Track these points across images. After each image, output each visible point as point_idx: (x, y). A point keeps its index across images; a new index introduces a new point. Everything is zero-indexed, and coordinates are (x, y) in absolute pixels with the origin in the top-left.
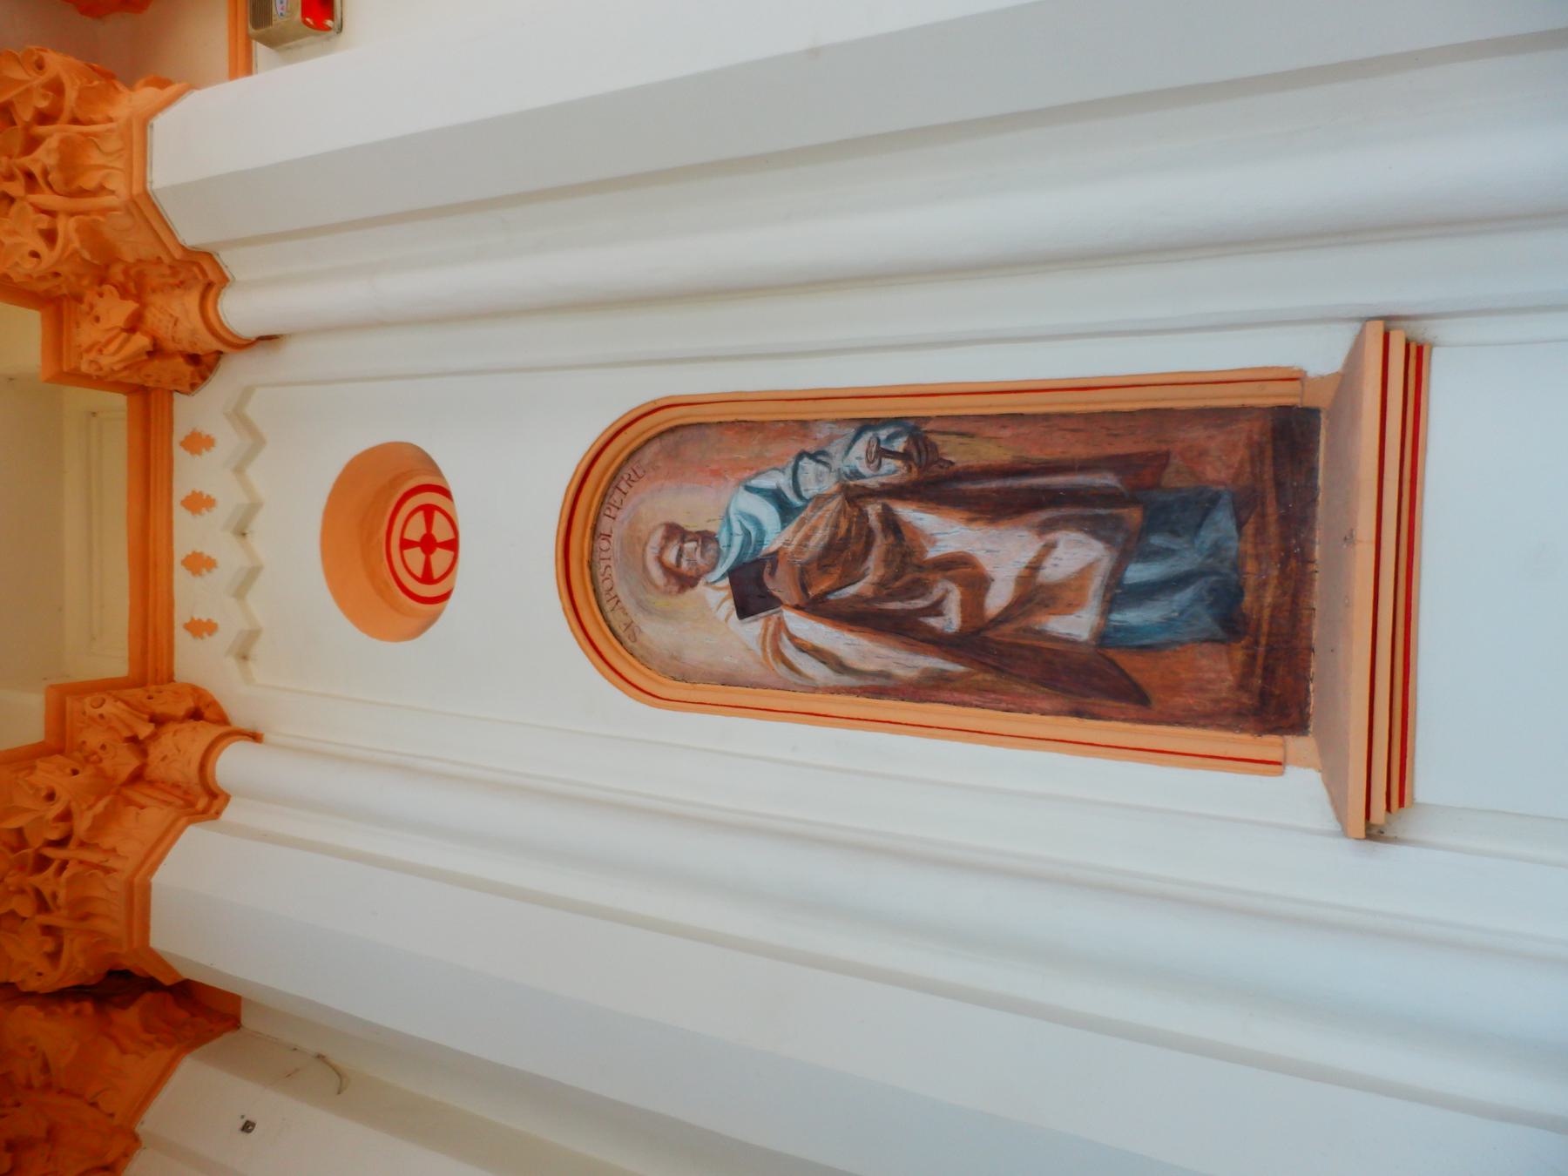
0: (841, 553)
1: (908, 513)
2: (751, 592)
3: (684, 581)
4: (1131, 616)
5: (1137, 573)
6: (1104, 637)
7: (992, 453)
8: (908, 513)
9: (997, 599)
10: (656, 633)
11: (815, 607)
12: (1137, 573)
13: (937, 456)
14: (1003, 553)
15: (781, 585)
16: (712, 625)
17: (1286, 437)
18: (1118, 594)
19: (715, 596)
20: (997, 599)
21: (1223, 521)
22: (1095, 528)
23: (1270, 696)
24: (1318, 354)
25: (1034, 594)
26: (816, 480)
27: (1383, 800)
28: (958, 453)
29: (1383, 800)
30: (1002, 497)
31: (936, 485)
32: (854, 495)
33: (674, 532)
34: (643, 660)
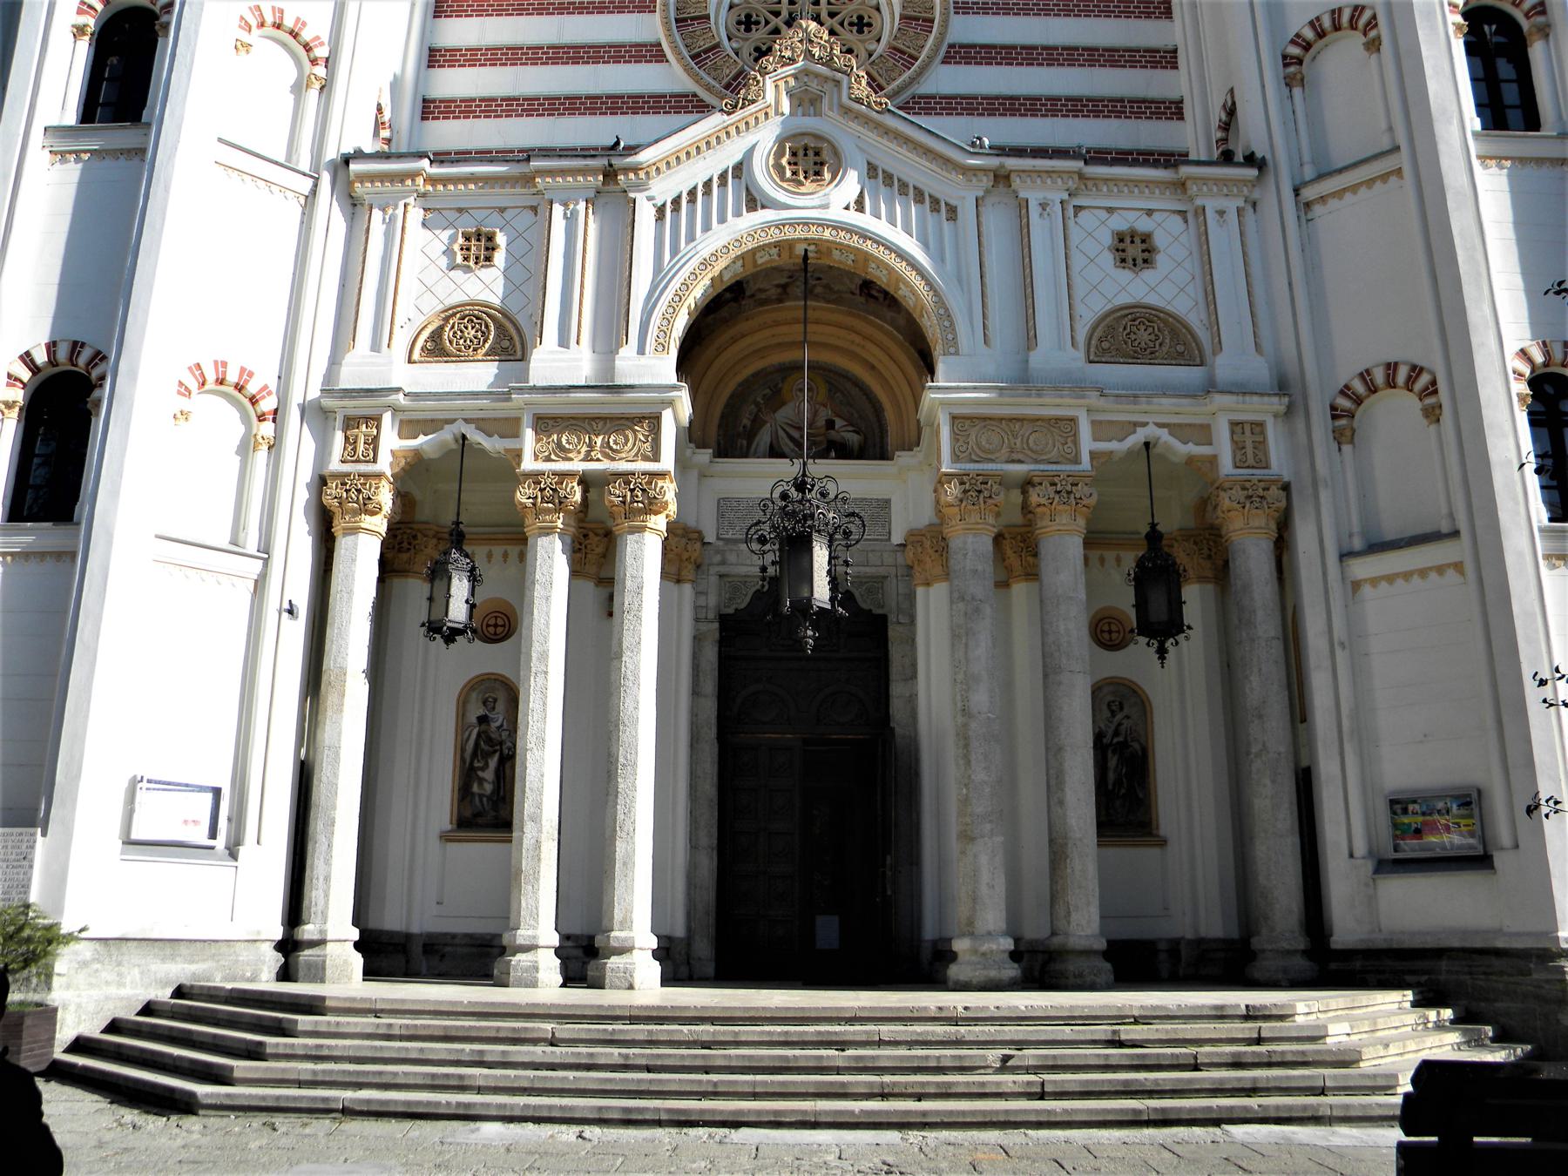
0: (489, 740)
2: (483, 720)
3: (485, 703)
6: (473, 794)
7: (508, 771)
8: (497, 756)
10: (474, 695)
11: (479, 735)
14: (489, 775)
15: (484, 727)
16: (475, 711)
18: (481, 796)
19: (481, 711)
21: (493, 813)
25: (481, 781)
26: (505, 735)
27: (446, 838)
28: (508, 765)
29: (446, 838)
32: (501, 743)
33: (495, 700)
34: (468, 694)
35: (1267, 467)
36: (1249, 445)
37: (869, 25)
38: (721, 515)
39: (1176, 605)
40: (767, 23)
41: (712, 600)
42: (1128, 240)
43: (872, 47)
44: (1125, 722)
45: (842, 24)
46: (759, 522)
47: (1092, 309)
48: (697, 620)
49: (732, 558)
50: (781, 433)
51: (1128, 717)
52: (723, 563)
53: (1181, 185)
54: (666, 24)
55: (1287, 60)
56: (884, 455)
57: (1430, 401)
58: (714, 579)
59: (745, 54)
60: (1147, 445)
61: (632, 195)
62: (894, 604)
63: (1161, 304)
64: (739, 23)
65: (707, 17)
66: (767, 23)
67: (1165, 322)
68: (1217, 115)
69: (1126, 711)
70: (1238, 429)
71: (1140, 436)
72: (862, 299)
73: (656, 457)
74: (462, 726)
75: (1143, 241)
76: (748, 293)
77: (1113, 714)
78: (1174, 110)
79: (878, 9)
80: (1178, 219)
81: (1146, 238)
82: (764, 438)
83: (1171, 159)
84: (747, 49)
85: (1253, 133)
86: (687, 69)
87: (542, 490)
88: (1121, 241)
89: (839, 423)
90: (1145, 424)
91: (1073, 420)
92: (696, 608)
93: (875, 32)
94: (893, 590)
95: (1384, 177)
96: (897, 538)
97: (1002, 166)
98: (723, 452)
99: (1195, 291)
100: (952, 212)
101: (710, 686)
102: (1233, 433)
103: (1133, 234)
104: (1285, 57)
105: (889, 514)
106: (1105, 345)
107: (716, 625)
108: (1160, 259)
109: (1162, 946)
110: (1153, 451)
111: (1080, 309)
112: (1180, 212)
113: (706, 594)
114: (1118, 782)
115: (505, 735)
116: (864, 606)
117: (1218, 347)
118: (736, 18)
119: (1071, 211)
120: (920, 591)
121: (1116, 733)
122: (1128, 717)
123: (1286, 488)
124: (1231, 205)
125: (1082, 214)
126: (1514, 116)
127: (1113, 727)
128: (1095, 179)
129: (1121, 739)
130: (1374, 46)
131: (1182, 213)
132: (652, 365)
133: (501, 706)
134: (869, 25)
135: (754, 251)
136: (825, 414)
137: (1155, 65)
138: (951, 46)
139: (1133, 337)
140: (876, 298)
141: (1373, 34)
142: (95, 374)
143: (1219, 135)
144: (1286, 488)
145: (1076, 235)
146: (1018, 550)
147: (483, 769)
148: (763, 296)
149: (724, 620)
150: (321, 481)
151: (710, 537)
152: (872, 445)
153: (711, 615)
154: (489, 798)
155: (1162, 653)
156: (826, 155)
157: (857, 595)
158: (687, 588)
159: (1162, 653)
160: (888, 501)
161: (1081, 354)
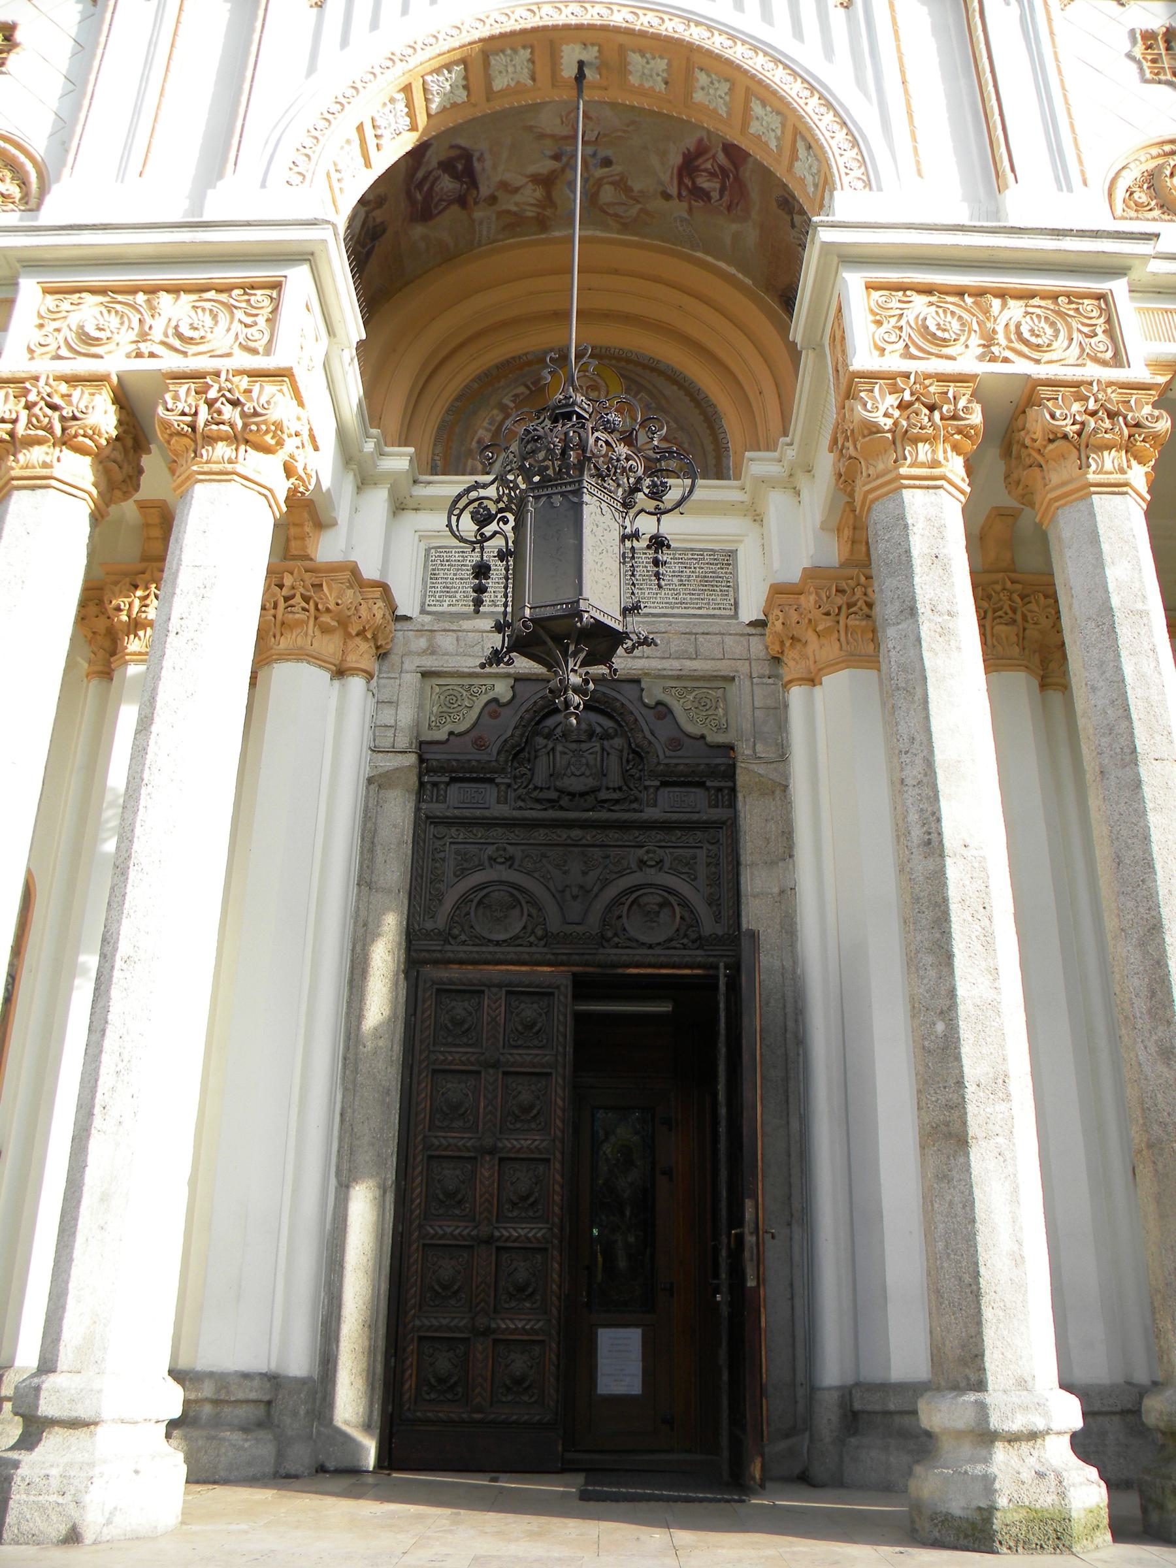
41: (406, 716)
49: (446, 642)
52: (431, 651)
58: (411, 679)
62: (747, 726)
72: (679, 209)
76: (484, 191)
87: (29, 406)
92: (377, 728)
94: (745, 701)
105: (735, 574)
107: (411, 759)
113: (393, 703)
116: (690, 728)
120: (796, 695)
140: (704, 195)
148: (509, 203)
149: (423, 748)
151: (407, 603)
153: (403, 742)
157: (677, 707)
158: (357, 684)
160: (732, 554)
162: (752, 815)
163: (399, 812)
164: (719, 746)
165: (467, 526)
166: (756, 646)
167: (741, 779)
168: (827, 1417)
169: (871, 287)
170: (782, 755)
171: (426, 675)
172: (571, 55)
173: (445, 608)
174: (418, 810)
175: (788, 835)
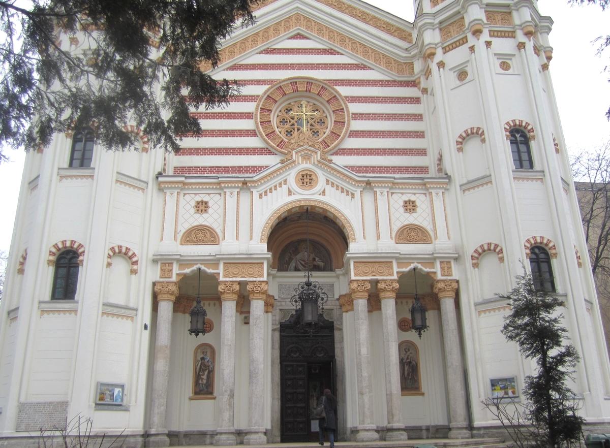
0: (205, 366)
1: (207, 371)
2: (202, 359)
4: (201, 385)
5: (204, 385)
6: (200, 384)
8: (207, 371)
9: (202, 377)
11: (201, 363)
12: (204, 385)
13: (211, 372)
14: (205, 377)
15: (203, 361)
16: (200, 356)
17: (211, 393)
18: (202, 384)
19: (202, 356)
20: (202, 377)
22: (206, 383)
23: (196, 393)
24: (215, 394)
25: (202, 379)
27: (191, 399)
28: (211, 373)
29: (191, 399)
30: (208, 377)
31: (209, 372)
35: (451, 275)
36: (446, 269)
37: (324, 123)
38: (280, 290)
39: (424, 319)
40: (290, 122)
41: (277, 318)
42: (408, 203)
43: (325, 131)
44: (410, 355)
45: (315, 122)
46: (295, 296)
47: (397, 226)
48: (273, 324)
49: (283, 303)
50: (298, 263)
51: (411, 353)
52: (281, 305)
53: (425, 184)
54: (256, 123)
55: (458, 143)
56: (331, 270)
57: (500, 255)
58: (278, 311)
59: (283, 133)
60: (414, 269)
61: (252, 190)
63: (418, 224)
64: (281, 122)
65: (270, 121)
66: (290, 122)
67: (420, 229)
68: (437, 156)
69: (410, 352)
70: (443, 264)
71: (412, 266)
73: (262, 276)
74: (195, 360)
75: (413, 203)
77: (406, 352)
78: (422, 152)
79: (327, 117)
80: (424, 196)
81: (413, 202)
82: (293, 265)
83: (424, 169)
84: (283, 131)
85: (448, 166)
86: (264, 140)
88: (406, 203)
89: (317, 259)
90: (413, 263)
91: (391, 262)
92: (273, 320)
93: (326, 125)
94: (336, 313)
95: (487, 183)
96: (337, 296)
97: (368, 180)
98: (280, 270)
99: (429, 219)
100: (353, 194)
101: (277, 346)
102: (441, 265)
103: (409, 201)
104: (457, 142)
105: (334, 289)
106: (401, 238)
107: (279, 326)
108: (418, 210)
109: (424, 428)
110: (416, 271)
111: (393, 226)
112: (424, 194)
114: (408, 375)
115: (210, 363)
116: (326, 319)
117: (436, 238)
118: (280, 120)
119: (390, 194)
120: (344, 314)
121: (407, 358)
122: (411, 353)
123: (458, 282)
124: (440, 191)
125: (394, 195)
126: (526, 164)
127: (406, 356)
128: (398, 184)
129: (409, 360)
130: (483, 141)
131: (425, 194)
132: (260, 248)
133: (209, 354)
134: (324, 123)
135: (291, 209)
136: (312, 256)
137: (417, 137)
138: (351, 131)
139: (410, 234)
141: (483, 137)
142: (80, 251)
143: (438, 162)
144: (458, 282)
145: (392, 202)
146: (374, 302)
147: (203, 375)
150: (154, 284)
151: (276, 297)
152: (328, 266)
153: (277, 323)
154: (205, 385)
155: (420, 334)
156: (313, 177)
158: (270, 314)
159: (420, 334)
161: (393, 241)
162: (337, 334)
163: (277, 334)
164: (331, 322)
165: (294, 303)
166: (337, 303)
167: (334, 328)
168: (348, 432)
169: (354, 262)
170: (342, 324)
171: (280, 310)
172: (305, 208)
173: (283, 297)
174: (280, 335)
175: (342, 338)
